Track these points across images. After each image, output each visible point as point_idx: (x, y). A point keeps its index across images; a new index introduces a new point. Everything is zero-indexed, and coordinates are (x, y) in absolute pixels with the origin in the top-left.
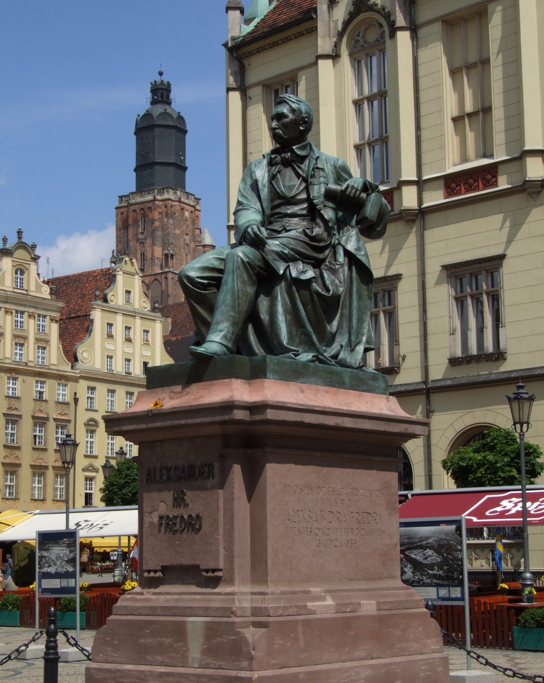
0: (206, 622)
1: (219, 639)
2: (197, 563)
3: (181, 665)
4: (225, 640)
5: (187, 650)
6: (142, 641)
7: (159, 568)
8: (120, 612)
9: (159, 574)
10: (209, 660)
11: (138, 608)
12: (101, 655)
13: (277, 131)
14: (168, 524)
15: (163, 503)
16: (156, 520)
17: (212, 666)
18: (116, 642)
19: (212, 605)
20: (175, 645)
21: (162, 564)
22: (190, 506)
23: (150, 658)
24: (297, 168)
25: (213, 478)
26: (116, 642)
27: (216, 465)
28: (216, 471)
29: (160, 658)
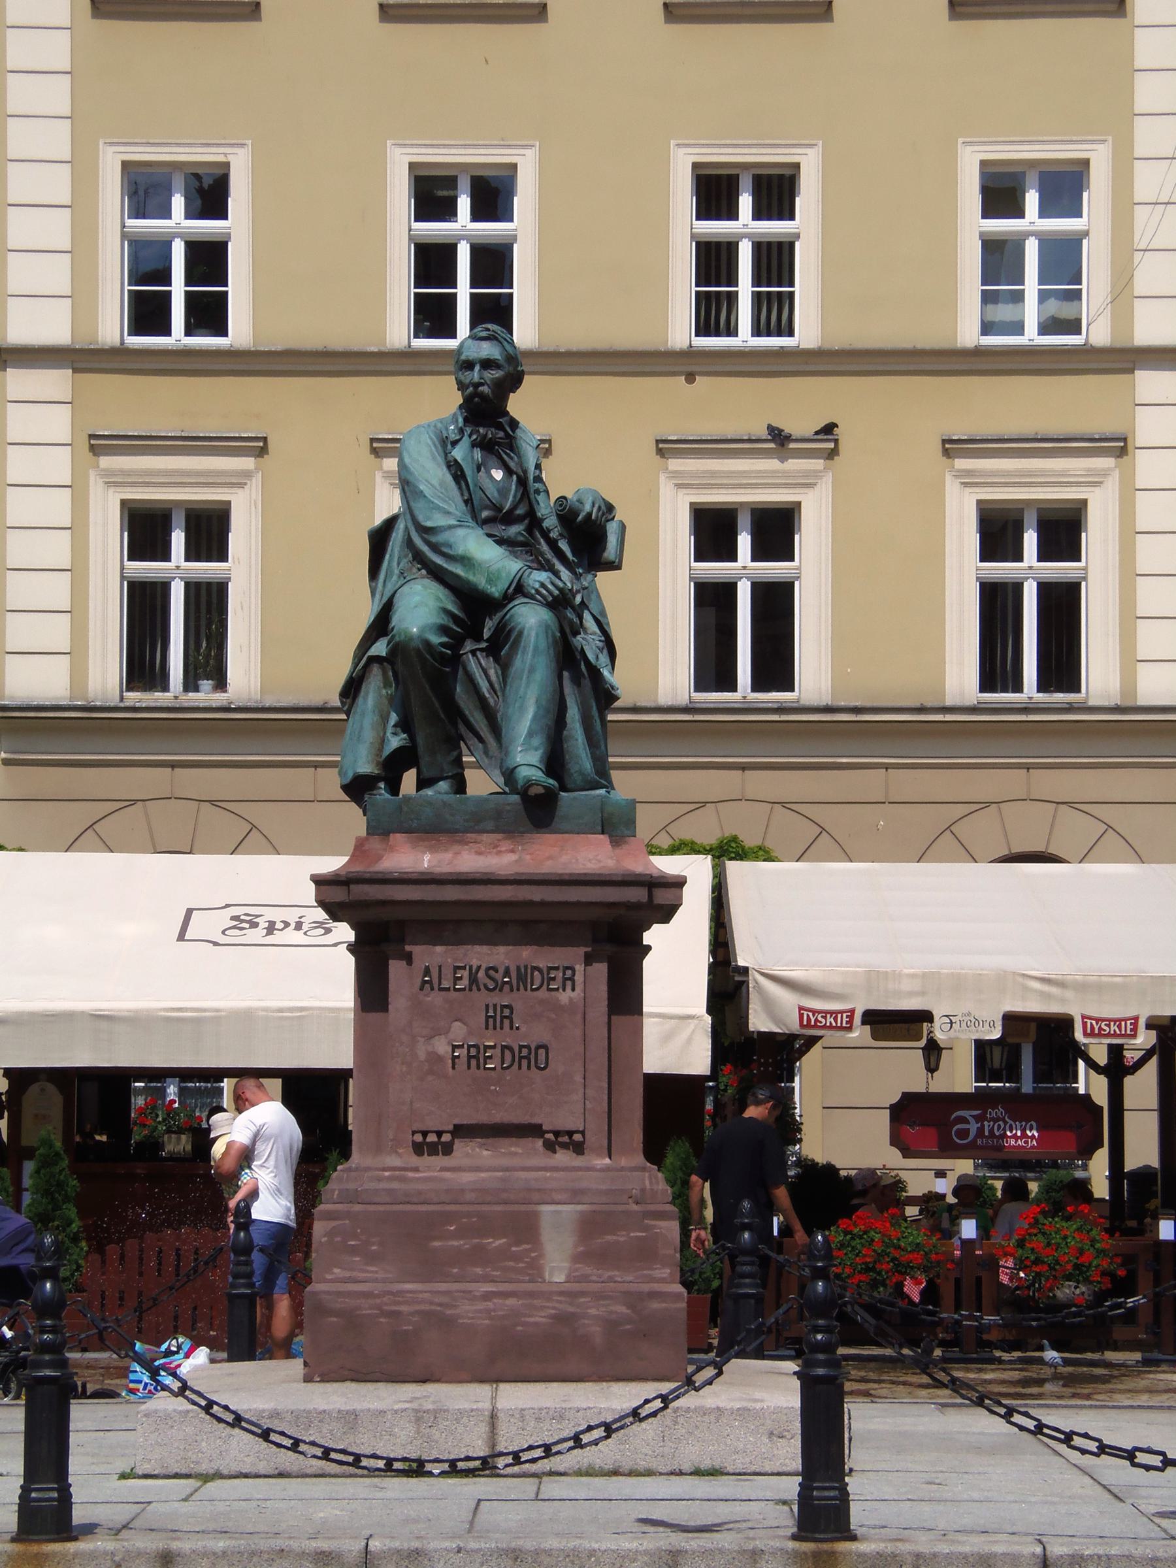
0: (581, 1212)
1: (609, 1238)
2: (536, 1120)
3: (527, 1278)
4: (622, 1239)
5: (541, 1256)
6: (437, 1244)
7: (451, 1128)
8: (377, 1200)
9: (446, 1138)
10: (588, 1270)
11: (420, 1193)
12: (336, 1270)
13: (485, 389)
14: (470, 1058)
15: (457, 1024)
16: (442, 1047)
17: (594, 1278)
18: (374, 1248)
19: (584, 1184)
20: (514, 1249)
21: (457, 1121)
22: (523, 1029)
23: (455, 1270)
24: (505, 456)
25: (573, 990)
26: (374, 1248)
27: (579, 968)
28: (579, 978)
29: (479, 1271)
